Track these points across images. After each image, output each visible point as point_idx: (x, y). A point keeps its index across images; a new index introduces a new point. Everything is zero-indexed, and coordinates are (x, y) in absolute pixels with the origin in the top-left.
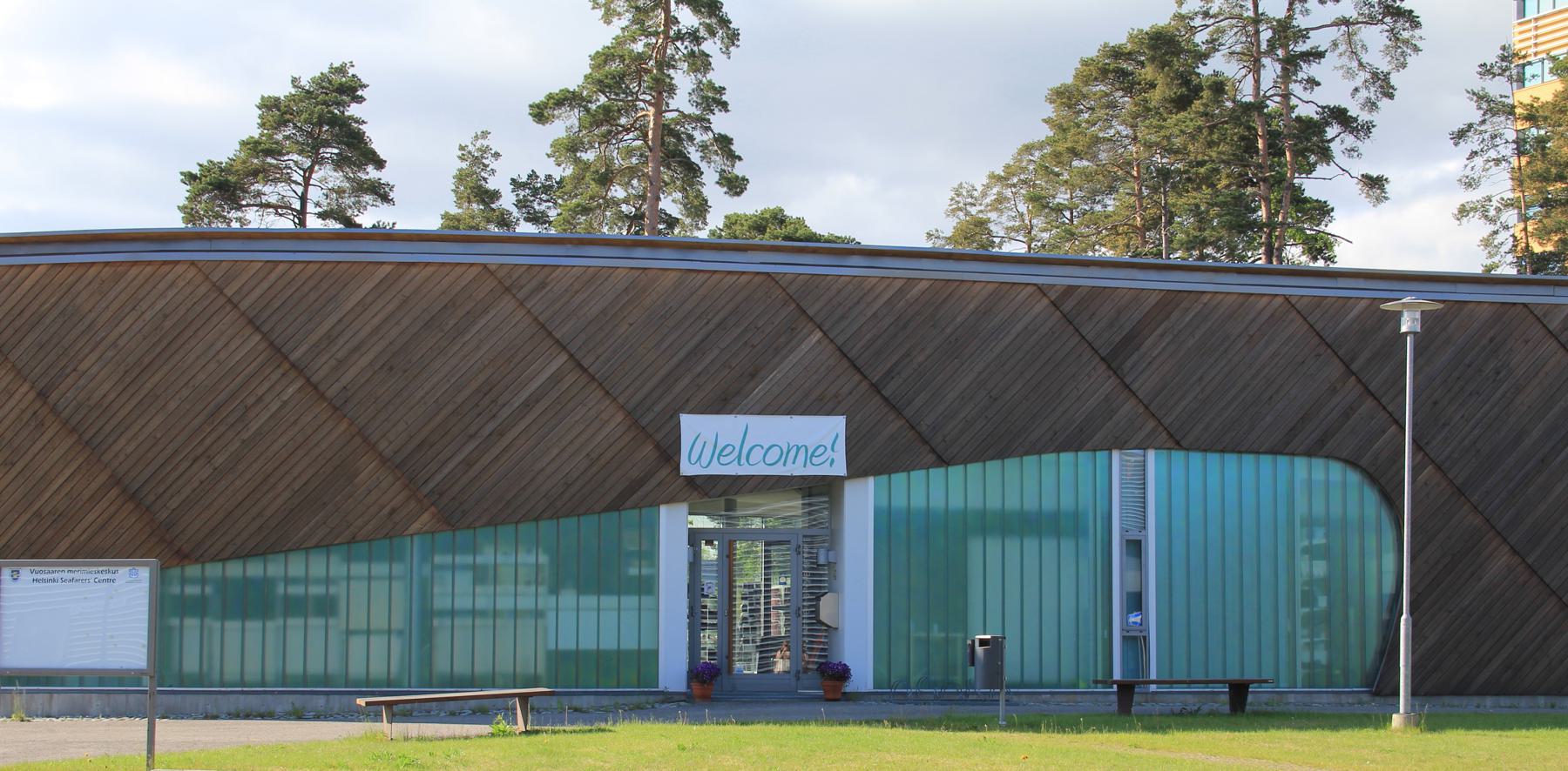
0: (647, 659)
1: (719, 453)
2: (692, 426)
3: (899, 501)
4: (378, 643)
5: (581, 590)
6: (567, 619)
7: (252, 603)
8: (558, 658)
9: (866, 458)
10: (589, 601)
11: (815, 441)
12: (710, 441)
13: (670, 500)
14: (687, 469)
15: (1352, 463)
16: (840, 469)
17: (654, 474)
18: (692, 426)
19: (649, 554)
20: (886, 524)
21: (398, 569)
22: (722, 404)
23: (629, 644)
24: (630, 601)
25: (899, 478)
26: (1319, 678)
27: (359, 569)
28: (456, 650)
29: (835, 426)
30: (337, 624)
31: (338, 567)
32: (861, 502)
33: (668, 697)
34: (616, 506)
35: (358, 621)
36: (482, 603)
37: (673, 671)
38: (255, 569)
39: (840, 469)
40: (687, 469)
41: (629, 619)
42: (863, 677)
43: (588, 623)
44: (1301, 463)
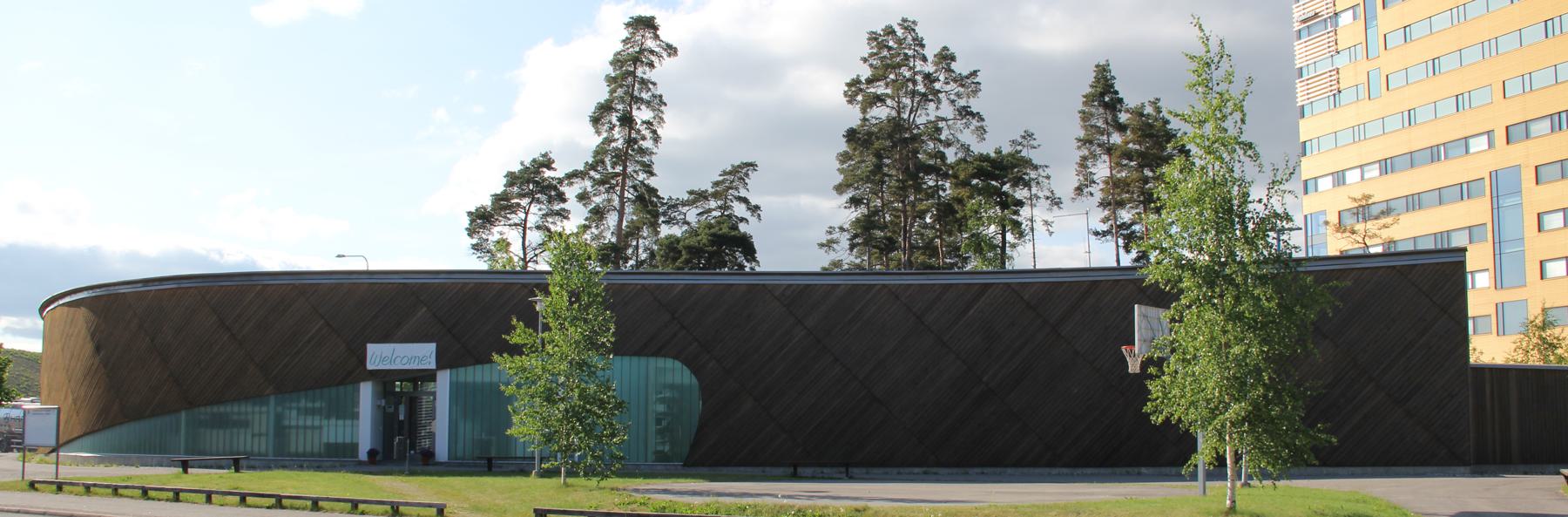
0: (354, 447)
1: (383, 360)
2: (372, 348)
3: (462, 379)
4: (263, 439)
5: (338, 418)
6: (332, 430)
7: (222, 422)
8: (328, 445)
9: (444, 361)
10: (340, 422)
11: (421, 355)
12: (381, 355)
13: (364, 380)
14: (370, 367)
15: (675, 358)
16: (433, 366)
17: (356, 370)
18: (372, 348)
19: (356, 403)
20: (457, 390)
21: (264, 409)
22: (386, 336)
23: (348, 440)
24: (348, 422)
25: (462, 370)
26: (661, 457)
27: (257, 409)
28: (297, 443)
29: (432, 347)
30: (249, 431)
31: (250, 409)
32: (444, 379)
33: (361, 463)
34: (342, 383)
35: (256, 431)
36: (301, 423)
37: (363, 455)
38: (222, 409)
39: (433, 366)
40: (370, 367)
41: (348, 430)
42: (442, 451)
43: (334, 431)
44: (652, 360)
